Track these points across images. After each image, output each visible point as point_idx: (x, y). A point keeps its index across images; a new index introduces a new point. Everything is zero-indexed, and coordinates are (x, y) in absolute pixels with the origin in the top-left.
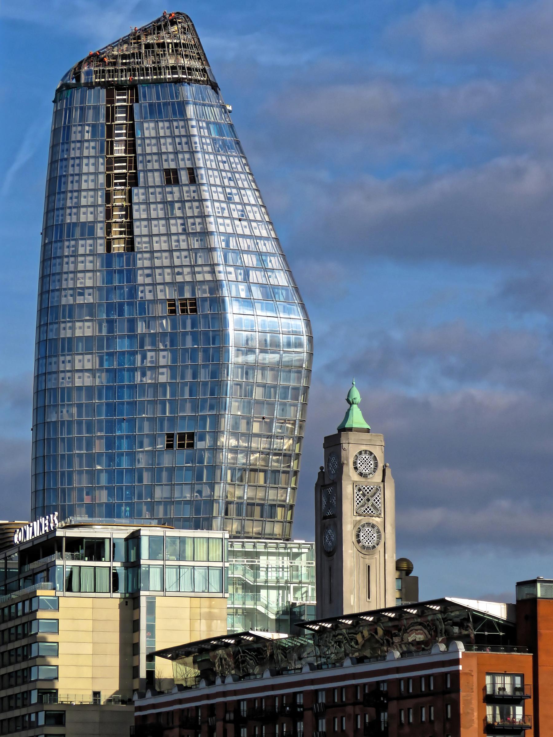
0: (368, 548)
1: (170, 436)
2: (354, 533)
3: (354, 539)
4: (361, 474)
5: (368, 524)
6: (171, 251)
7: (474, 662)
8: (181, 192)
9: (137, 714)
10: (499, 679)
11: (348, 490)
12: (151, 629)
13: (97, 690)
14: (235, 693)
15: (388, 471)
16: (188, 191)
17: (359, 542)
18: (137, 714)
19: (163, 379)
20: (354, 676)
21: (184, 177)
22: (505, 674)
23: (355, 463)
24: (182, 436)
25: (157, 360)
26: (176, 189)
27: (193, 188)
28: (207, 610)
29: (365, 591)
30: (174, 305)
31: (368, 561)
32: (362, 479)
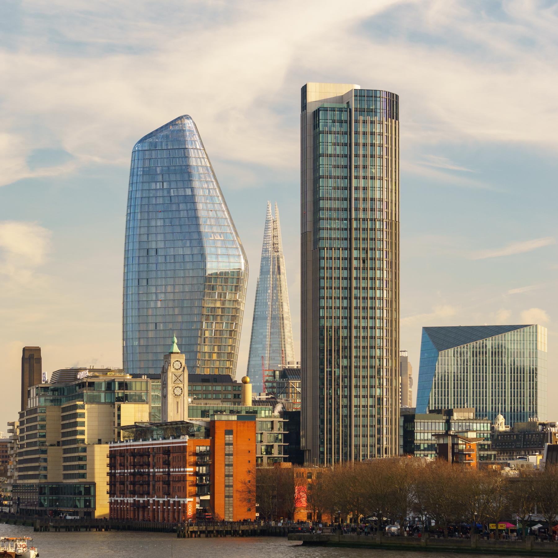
2: (172, 390)
3: (172, 393)
7: (192, 442)
11: (170, 375)
12: (119, 417)
13: (100, 438)
14: (133, 446)
15: (186, 368)
20: (162, 444)
22: (203, 446)
31: (177, 400)
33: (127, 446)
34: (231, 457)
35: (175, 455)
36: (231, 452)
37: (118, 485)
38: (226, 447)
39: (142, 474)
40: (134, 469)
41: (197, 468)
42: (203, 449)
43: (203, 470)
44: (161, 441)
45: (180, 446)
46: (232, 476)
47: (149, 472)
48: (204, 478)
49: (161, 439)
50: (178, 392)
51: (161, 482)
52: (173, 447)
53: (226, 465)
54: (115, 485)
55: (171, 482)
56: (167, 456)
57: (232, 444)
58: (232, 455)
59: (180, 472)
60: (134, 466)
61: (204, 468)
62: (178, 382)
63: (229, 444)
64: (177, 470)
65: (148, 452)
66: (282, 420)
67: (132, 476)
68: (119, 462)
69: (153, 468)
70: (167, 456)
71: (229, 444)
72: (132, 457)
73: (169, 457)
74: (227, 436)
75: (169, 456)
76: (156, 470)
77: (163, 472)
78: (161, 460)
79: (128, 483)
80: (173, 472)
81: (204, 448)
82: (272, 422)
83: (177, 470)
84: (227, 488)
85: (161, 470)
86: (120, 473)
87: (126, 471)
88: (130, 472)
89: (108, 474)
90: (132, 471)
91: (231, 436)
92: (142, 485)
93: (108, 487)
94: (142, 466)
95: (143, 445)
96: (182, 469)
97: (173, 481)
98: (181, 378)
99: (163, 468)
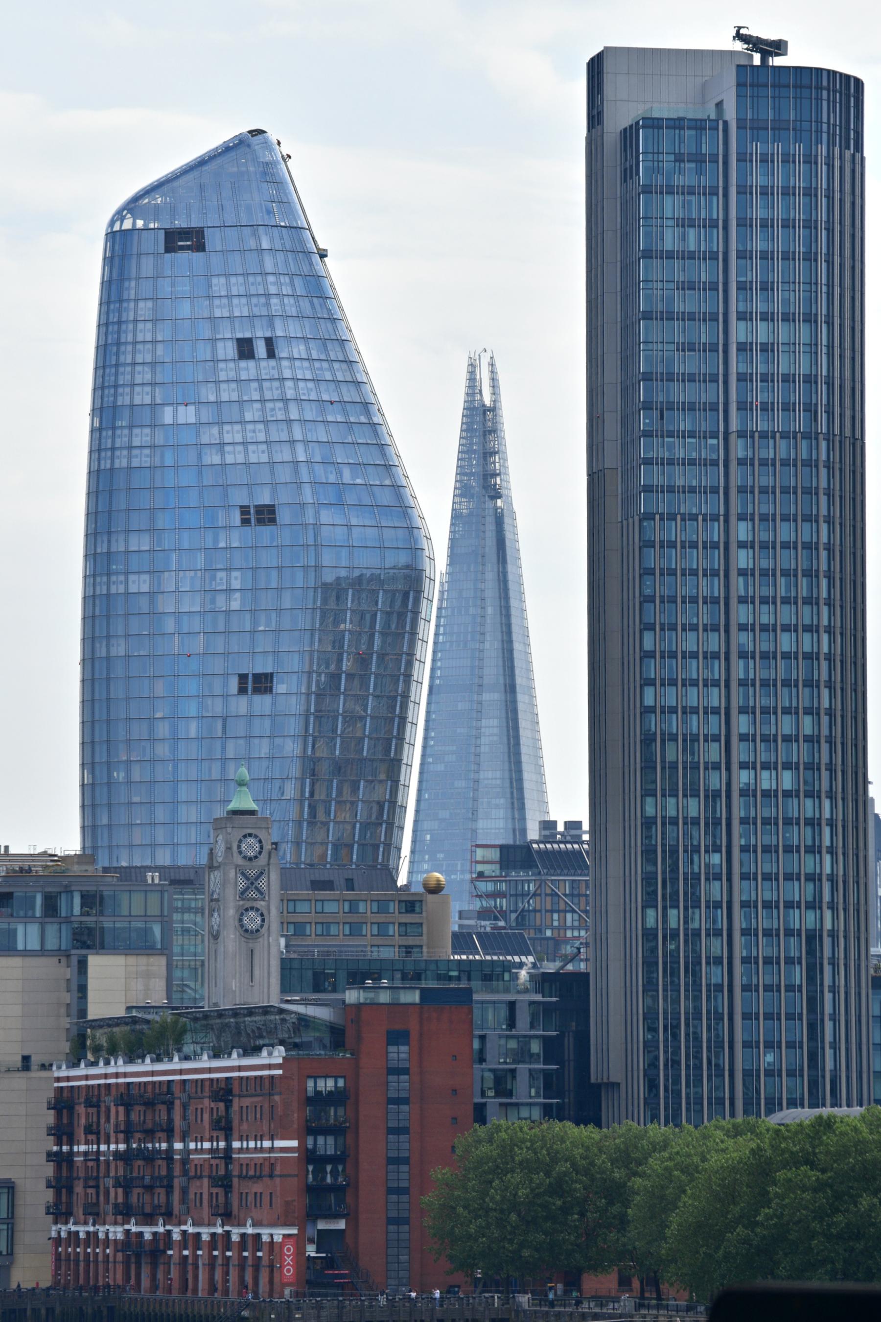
0: (252, 932)
1: (243, 678)
2: (237, 917)
4: (245, 857)
5: (252, 908)
6: (244, 444)
8: (258, 368)
9: (56, 1085)
10: (321, 1084)
13: (26, 1053)
14: (125, 1075)
16: (267, 367)
17: (242, 926)
18: (56, 1085)
19: (235, 605)
20: (210, 1070)
21: (261, 349)
22: (326, 1077)
23: (239, 847)
24: (257, 677)
25: (229, 582)
26: (251, 364)
27: (272, 363)
28: (144, 968)
29: (248, 975)
30: (248, 513)
31: (251, 945)
32: (248, 863)
33: (106, 1076)
34: (405, 1108)
35: (246, 1102)
36: (403, 1095)
37: (79, 1189)
38: (390, 1078)
39: (150, 1157)
40: (127, 1141)
41: (310, 1141)
42: (327, 1085)
43: (327, 1145)
44: (205, 1062)
45: (261, 1077)
46: (406, 1161)
47: (170, 1151)
48: (329, 1168)
49: (205, 1057)
50: (252, 921)
51: (206, 1181)
52: (241, 1078)
53: (391, 1131)
54: (70, 1190)
55: (235, 1181)
56: (222, 1105)
57: (406, 1071)
58: (406, 1101)
59: (262, 1150)
60: (128, 1134)
61: (331, 1140)
62: (253, 894)
63: (398, 1071)
64: (252, 1144)
65: (169, 1092)
66: (538, 998)
67: (120, 1164)
68: (83, 1121)
69: (183, 1140)
70: (222, 1105)
71: (398, 1071)
72: (121, 1109)
73: (227, 1108)
74: (392, 1049)
75: (228, 1104)
76: (192, 1146)
77: (211, 1151)
78: (206, 1117)
79: (110, 1182)
80: (241, 1150)
81: (330, 1083)
82: (512, 1005)
83: (252, 1144)
84: (394, 1198)
85: (207, 1145)
86: (86, 1154)
87: (103, 1147)
88: (116, 1153)
89: (50, 1155)
90: (122, 1147)
91: (404, 1048)
92: (150, 1188)
93: (49, 1195)
94: (150, 1134)
95: (153, 1073)
96: (267, 1144)
97: (240, 1177)
98: (262, 883)
99: (211, 1140)
